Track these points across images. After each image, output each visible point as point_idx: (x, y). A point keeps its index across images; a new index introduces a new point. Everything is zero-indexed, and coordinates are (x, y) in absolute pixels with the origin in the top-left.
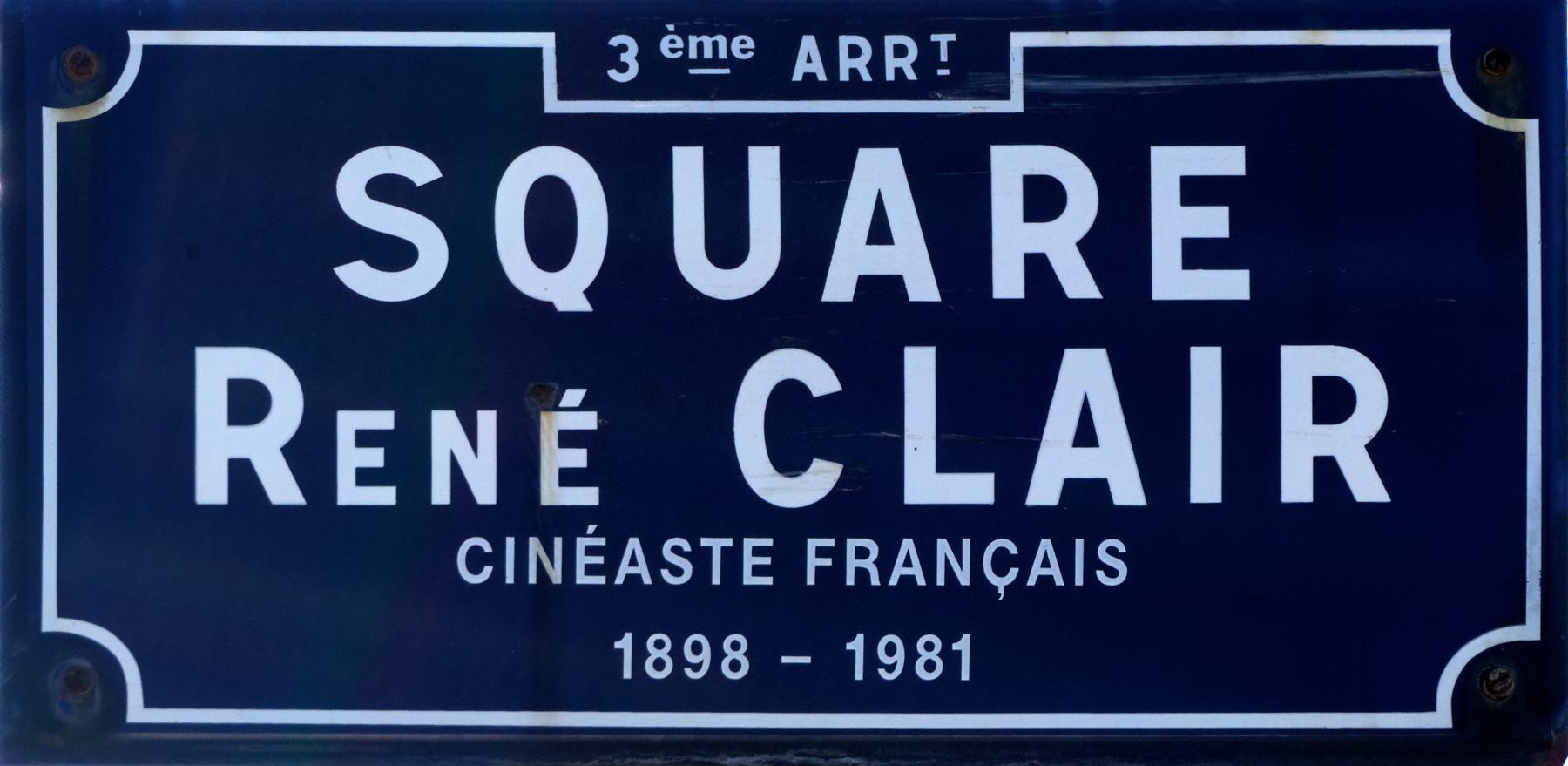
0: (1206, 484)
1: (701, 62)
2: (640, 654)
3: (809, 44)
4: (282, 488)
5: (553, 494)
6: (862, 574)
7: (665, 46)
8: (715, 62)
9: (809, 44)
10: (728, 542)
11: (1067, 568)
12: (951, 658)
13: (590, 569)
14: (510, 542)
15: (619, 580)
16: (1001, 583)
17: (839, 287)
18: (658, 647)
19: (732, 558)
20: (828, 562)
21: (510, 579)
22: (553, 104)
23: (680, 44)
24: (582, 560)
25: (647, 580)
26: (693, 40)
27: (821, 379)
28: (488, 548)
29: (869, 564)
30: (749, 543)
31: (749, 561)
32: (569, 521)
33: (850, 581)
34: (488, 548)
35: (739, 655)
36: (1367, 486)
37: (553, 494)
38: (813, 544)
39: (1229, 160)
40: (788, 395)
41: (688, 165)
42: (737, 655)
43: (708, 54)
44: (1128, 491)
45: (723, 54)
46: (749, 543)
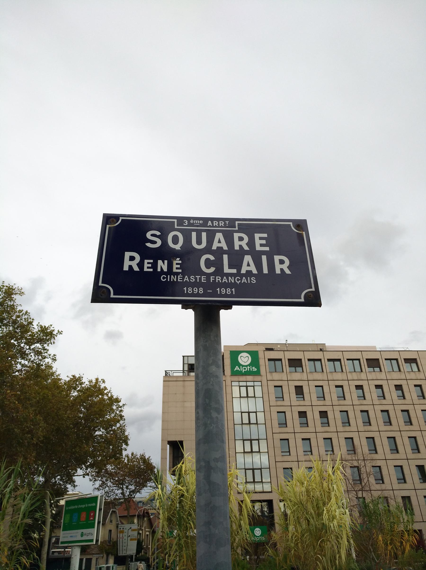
0: (265, 271)
1: (196, 223)
2: (187, 290)
3: (210, 222)
4: (136, 269)
5: (175, 270)
6: (219, 281)
7: (191, 221)
8: (198, 223)
9: (210, 222)
10: (200, 277)
11: (247, 281)
12: (232, 292)
13: (180, 279)
14: (169, 276)
15: (184, 281)
16: (238, 282)
17: (214, 247)
18: (190, 289)
19: (200, 279)
20: (214, 279)
21: (169, 280)
22: (176, 227)
23: (193, 221)
24: (179, 278)
25: (188, 281)
26: (195, 221)
27: (212, 258)
28: (166, 277)
29: (219, 280)
30: (203, 277)
31: (203, 279)
32: (178, 274)
33: (217, 282)
34: (166, 277)
35: (202, 290)
36: (288, 272)
37: (175, 270)
38: (211, 277)
39: (265, 235)
40: (207, 260)
41: (194, 234)
42: (201, 290)
43: (197, 222)
44: (255, 271)
45: (199, 223)
46: (203, 277)
